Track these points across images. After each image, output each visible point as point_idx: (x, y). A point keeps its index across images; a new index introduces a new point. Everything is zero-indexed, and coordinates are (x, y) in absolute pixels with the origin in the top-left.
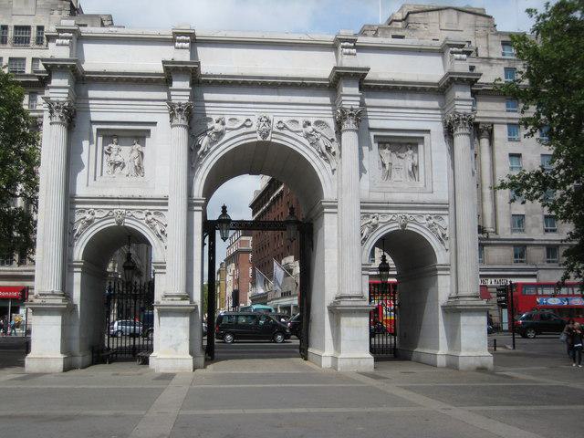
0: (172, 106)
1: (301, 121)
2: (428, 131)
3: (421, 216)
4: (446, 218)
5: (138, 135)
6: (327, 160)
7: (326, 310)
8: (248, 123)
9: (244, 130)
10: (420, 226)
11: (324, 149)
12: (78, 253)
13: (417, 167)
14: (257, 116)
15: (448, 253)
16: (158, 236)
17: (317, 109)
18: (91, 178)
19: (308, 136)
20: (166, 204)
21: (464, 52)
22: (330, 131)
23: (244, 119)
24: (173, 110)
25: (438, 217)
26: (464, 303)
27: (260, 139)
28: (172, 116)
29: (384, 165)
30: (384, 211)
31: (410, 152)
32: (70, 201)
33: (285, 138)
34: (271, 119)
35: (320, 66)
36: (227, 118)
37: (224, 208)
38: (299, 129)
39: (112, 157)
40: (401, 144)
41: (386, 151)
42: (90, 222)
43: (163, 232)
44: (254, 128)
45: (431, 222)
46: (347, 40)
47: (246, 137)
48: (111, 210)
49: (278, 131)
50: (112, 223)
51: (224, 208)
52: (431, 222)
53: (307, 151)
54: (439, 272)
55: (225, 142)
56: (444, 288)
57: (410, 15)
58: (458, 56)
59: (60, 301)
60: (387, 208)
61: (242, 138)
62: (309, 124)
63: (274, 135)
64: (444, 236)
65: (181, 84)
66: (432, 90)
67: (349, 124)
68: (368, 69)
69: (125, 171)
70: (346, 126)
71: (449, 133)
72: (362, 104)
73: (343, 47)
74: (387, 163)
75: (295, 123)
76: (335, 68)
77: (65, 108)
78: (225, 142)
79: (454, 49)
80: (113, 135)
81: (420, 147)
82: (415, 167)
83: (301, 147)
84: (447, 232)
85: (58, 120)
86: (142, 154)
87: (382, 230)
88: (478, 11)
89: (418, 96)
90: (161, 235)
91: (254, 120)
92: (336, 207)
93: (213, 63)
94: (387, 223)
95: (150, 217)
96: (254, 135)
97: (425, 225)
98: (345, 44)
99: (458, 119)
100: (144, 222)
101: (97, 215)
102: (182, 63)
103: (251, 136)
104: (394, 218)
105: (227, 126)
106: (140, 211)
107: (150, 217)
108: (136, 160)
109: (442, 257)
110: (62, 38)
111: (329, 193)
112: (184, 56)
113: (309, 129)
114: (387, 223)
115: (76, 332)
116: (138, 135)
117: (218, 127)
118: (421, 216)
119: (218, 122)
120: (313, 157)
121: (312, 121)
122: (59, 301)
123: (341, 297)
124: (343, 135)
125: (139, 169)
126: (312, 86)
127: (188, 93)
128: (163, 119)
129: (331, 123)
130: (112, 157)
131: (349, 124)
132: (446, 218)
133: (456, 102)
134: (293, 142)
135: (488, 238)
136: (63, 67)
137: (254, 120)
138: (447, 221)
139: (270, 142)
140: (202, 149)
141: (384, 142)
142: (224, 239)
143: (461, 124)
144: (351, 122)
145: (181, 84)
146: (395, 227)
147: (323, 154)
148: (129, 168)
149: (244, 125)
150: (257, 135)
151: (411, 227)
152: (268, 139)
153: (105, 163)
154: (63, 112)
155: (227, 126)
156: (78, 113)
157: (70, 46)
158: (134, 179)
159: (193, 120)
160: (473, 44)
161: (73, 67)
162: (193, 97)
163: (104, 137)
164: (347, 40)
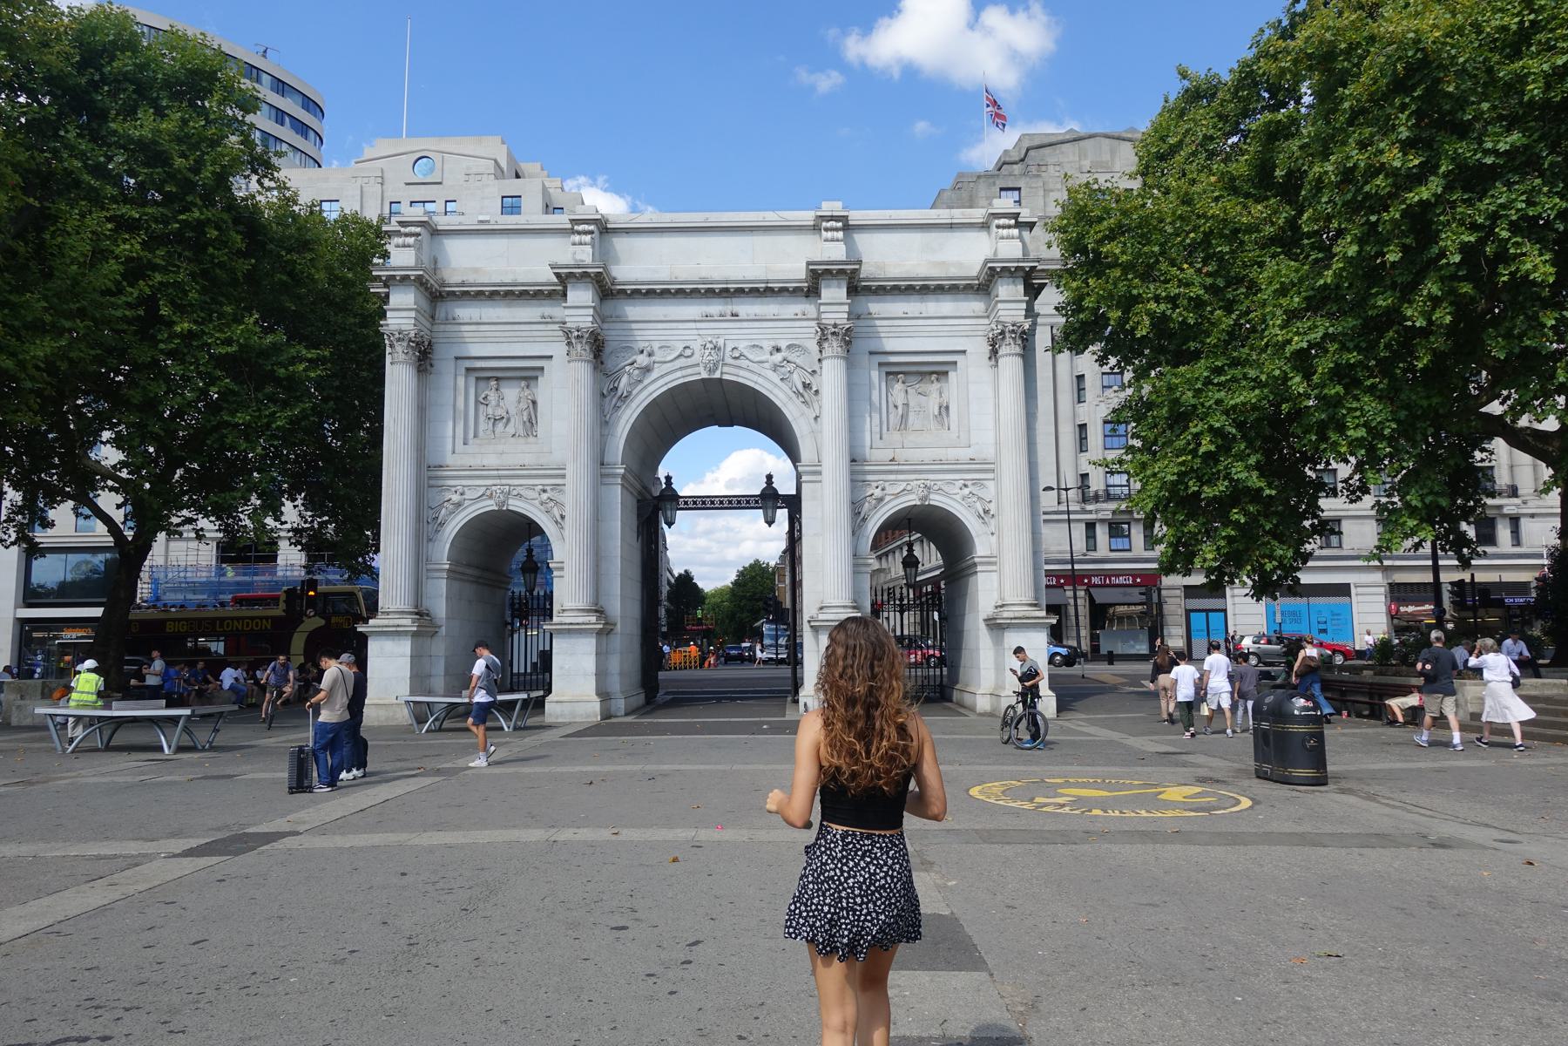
0: (567, 333)
1: (768, 346)
2: (964, 352)
3: (951, 482)
4: (991, 485)
5: (528, 375)
8: (688, 352)
9: (682, 362)
13: (947, 408)
14: (700, 342)
15: (994, 539)
17: (792, 324)
18: (459, 441)
19: (775, 368)
20: (563, 476)
21: (1018, 225)
22: (808, 362)
23: (680, 346)
25: (976, 482)
26: (1011, 615)
27: (705, 375)
28: (569, 344)
30: (892, 477)
31: (936, 386)
32: (428, 474)
33: (742, 373)
34: (721, 342)
35: (788, 259)
36: (656, 346)
38: (763, 358)
39: (490, 410)
41: (898, 387)
43: (563, 517)
44: (696, 359)
46: (832, 218)
47: (684, 372)
49: (729, 360)
50: (490, 505)
51: (668, 478)
52: (966, 491)
53: (776, 391)
57: (1032, 153)
58: (1005, 232)
59: (408, 622)
61: (679, 374)
62: (778, 350)
63: (726, 369)
64: (986, 512)
66: (968, 288)
67: (833, 347)
68: (860, 262)
69: (511, 429)
70: (828, 351)
71: (994, 353)
72: (854, 316)
73: (827, 230)
74: (900, 404)
75: (756, 349)
76: (808, 264)
79: (1002, 221)
80: (489, 376)
82: (945, 409)
83: (770, 386)
84: (992, 508)
85: (402, 357)
86: (534, 403)
89: (948, 297)
90: (560, 521)
92: (819, 473)
93: (637, 263)
94: (897, 495)
96: (696, 369)
97: (958, 497)
98: (829, 224)
99: (1002, 333)
101: (469, 495)
103: (690, 371)
107: (545, 496)
109: (982, 547)
110: (406, 235)
113: (778, 357)
114: (897, 495)
117: (642, 360)
118: (951, 482)
121: (783, 345)
124: (825, 363)
125: (531, 424)
126: (783, 290)
127: (591, 311)
128: (559, 349)
129: (812, 345)
132: (991, 485)
133: (1000, 306)
134: (755, 378)
136: (405, 278)
137: (696, 346)
138: (989, 491)
139: (720, 380)
141: (893, 373)
142: (670, 524)
143: (1008, 340)
144: (835, 344)
146: (912, 500)
147: (798, 394)
148: (516, 425)
150: (701, 369)
151: (936, 500)
152: (717, 375)
153: (482, 418)
157: (418, 248)
158: (522, 440)
159: (598, 349)
161: (419, 278)
162: (601, 317)
163: (478, 379)
164: (832, 218)
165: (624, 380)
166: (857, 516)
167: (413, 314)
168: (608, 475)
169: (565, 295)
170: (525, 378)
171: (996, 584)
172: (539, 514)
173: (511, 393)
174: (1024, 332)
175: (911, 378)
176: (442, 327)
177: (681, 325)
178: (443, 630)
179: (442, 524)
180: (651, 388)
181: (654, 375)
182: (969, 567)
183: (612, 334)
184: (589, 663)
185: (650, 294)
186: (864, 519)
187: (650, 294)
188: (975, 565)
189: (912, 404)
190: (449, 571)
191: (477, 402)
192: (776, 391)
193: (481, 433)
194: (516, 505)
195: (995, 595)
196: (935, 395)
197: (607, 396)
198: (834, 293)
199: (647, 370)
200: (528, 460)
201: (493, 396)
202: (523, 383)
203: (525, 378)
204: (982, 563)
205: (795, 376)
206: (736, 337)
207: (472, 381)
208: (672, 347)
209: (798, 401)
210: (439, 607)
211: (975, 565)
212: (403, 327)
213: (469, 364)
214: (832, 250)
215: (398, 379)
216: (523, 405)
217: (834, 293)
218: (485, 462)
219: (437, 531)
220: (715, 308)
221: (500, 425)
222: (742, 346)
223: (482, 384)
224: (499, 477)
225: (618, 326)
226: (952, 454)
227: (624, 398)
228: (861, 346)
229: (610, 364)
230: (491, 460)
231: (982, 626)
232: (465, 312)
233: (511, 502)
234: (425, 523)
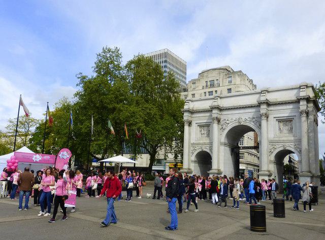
40: (287, 121)
113: (254, 120)
117: (228, 122)
131: (263, 118)
146: (282, 149)
149: (235, 120)
166: (271, 152)
169: (212, 111)
183: (222, 118)
194: (205, 150)
198: (264, 107)
208: (232, 119)
214: (263, 99)
215: (186, 128)
217: (264, 107)
220: (242, 111)
222: (247, 118)
227: (224, 129)
229: (222, 122)
230: (201, 142)
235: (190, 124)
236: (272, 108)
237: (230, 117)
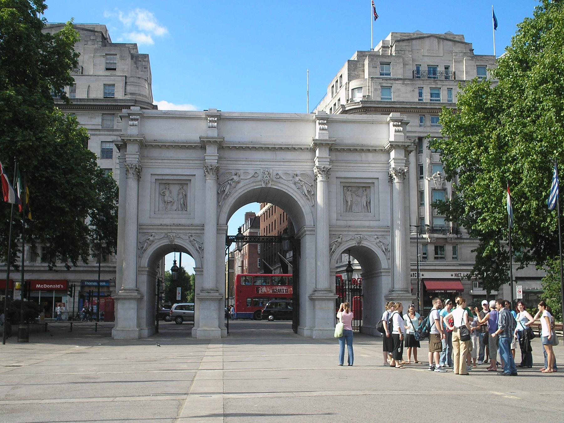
5: (184, 183)
6: (308, 199)
7: (307, 299)
9: (254, 178)
10: (370, 244)
11: (306, 192)
12: (145, 261)
14: (262, 171)
15: (390, 261)
16: (197, 250)
18: (152, 213)
19: (295, 183)
23: (252, 173)
24: (208, 169)
27: (264, 186)
29: (347, 202)
30: (346, 233)
32: (140, 227)
33: (280, 185)
37: (240, 229)
41: (349, 193)
42: (153, 241)
44: (259, 178)
45: (378, 240)
47: (254, 184)
48: (166, 234)
49: (275, 179)
50: (165, 242)
52: (378, 240)
53: (295, 194)
54: (383, 274)
55: (241, 188)
56: (385, 283)
58: (397, 128)
60: (349, 231)
61: (252, 185)
62: (297, 175)
63: (273, 183)
65: (212, 151)
69: (175, 207)
74: (349, 200)
77: (136, 168)
78: (241, 188)
80: (164, 183)
81: (372, 188)
82: (368, 204)
84: (390, 247)
87: (345, 246)
88: (457, 39)
91: (260, 172)
95: (192, 239)
96: (260, 183)
100: (188, 241)
102: (213, 138)
103: (258, 184)
104: (353, 238)
105: (241, 177)
106: (185, 234)
107: (192, 239)
108: (182, 200)
109: (384, 264)
110: (132, 120)
111: (308, 220)
112: (214, 133)
113: (297, 179)
115: (144, 313)
116: (184, 183)
117: (235, 178)
118: (370, 236)
119: (236, 175)
120: (299, 198)
121: (298, 173)
122: (135, 294)
123: (316, 291)
125: (184, 206)
128: (199, 173)
130: (166, 199)
134: (286, 187)
135: (461, 238)
137: (260, 172)
140: (226, 193)
145: (212, 151)
146: (353, 244)
149: (253, 176)
151: (365, 244)
152: (269, 186)
154: (135, 170)
155: (241, 177)
156: (143, 169)
160: (452, 69)
161: (141, 141)
165: (228, 187)
167: (137, 156)
168: (220, 230)
170: (181, 184)
171: (390, 281)
172: (188, 246)
173: (175, 189)
174: (404, 173)
175: (354, 189)
176: (146, 161)
177: (253, 163)
178: (145, 297)
179: (145, 250)
180: (240, 191)
181: (241, 185)
182: (378, 273)
184: (215, 315)
185: (241, 148)
186: (333, 252)
187: (241, 148)
188: (381, 272)
189: (354, 201)
190: (148, 271)
191: (160, 193)
192: (295, 194)
193: (161, 209)
194: (177, 242)
195: (390, 286)
196: (364, 197)
197: (221, 195)
199: (239, 182)
200: (183, 221)
201: (167, 193)
202: (181, 187)
203: (181, 184)
204: (384, 272)
205: (304, 187)
206: (278, 168)
207: (157, 186)
209: (304, 199)
210: (144, 288)
211: (381, 272)
212: (133, 162)
213: (157, 177)
216: (181, 196)
218: (165, 223)
219: (143, 253)
220: (268, 155)
221: (170, 204)
222: (280, 173)
223: (162, 186)
224: (171, 229)
225: (225, 162)
226: (373, 223)
228: (333, 175)
231: (383, 299)
232: (155, 153)
233: (176, 240)
234: (141, 250)
235: (139, 173)
236: (334, 156)
237: (241, 166)
